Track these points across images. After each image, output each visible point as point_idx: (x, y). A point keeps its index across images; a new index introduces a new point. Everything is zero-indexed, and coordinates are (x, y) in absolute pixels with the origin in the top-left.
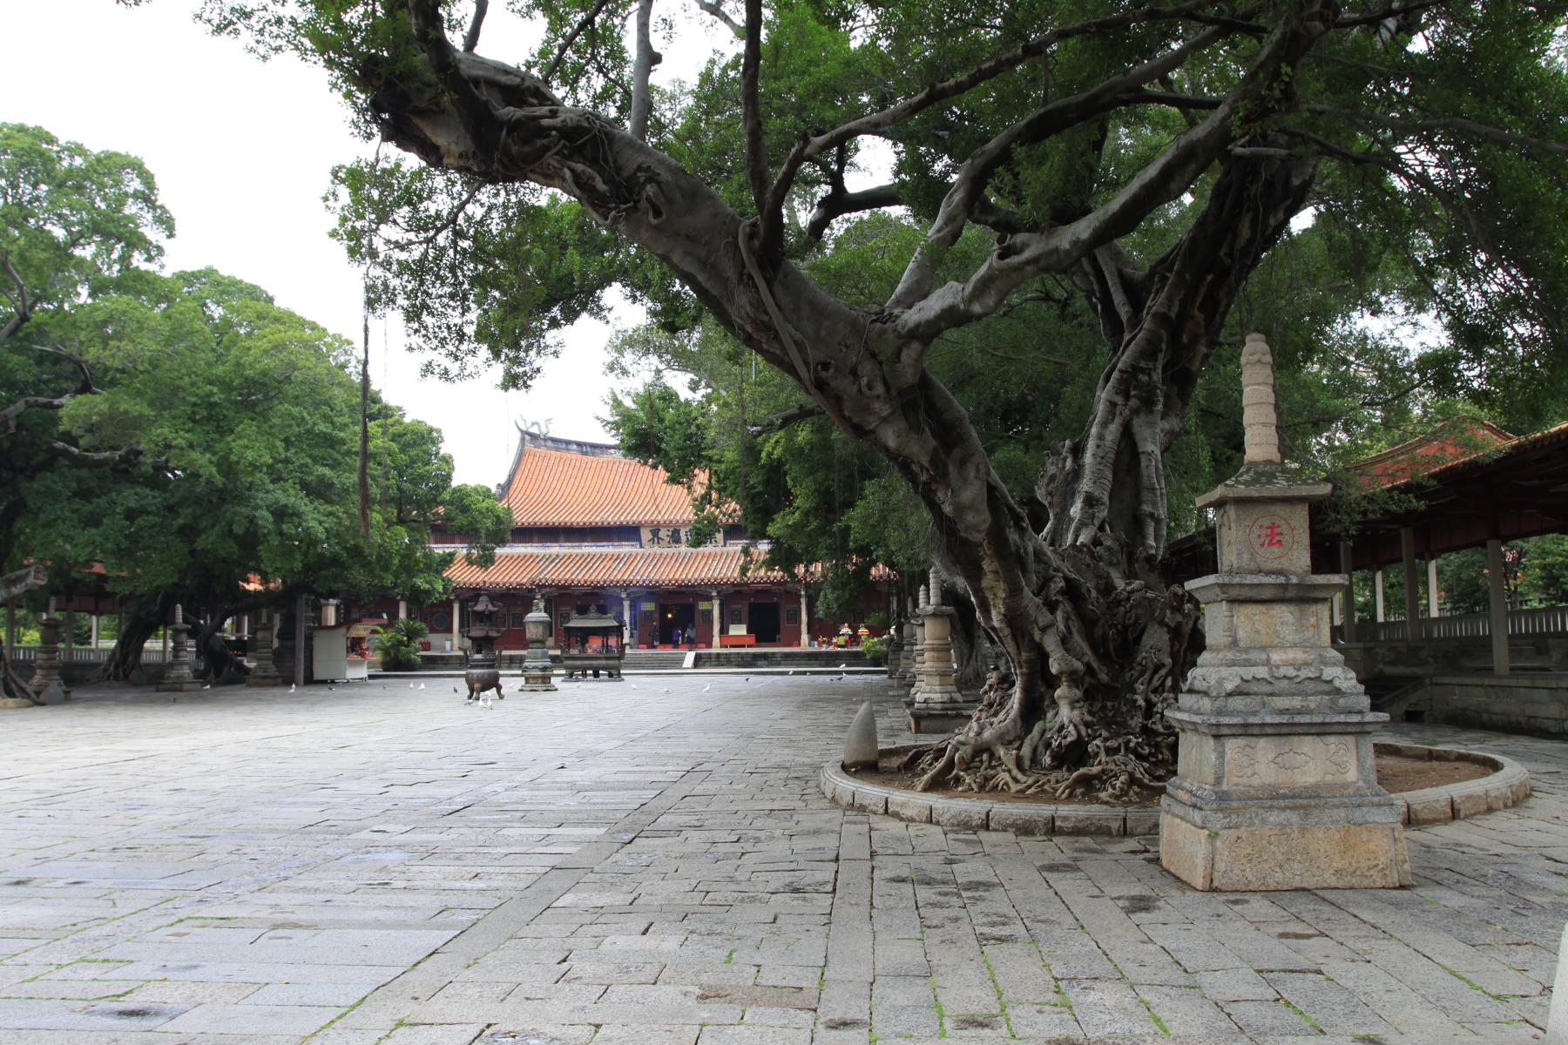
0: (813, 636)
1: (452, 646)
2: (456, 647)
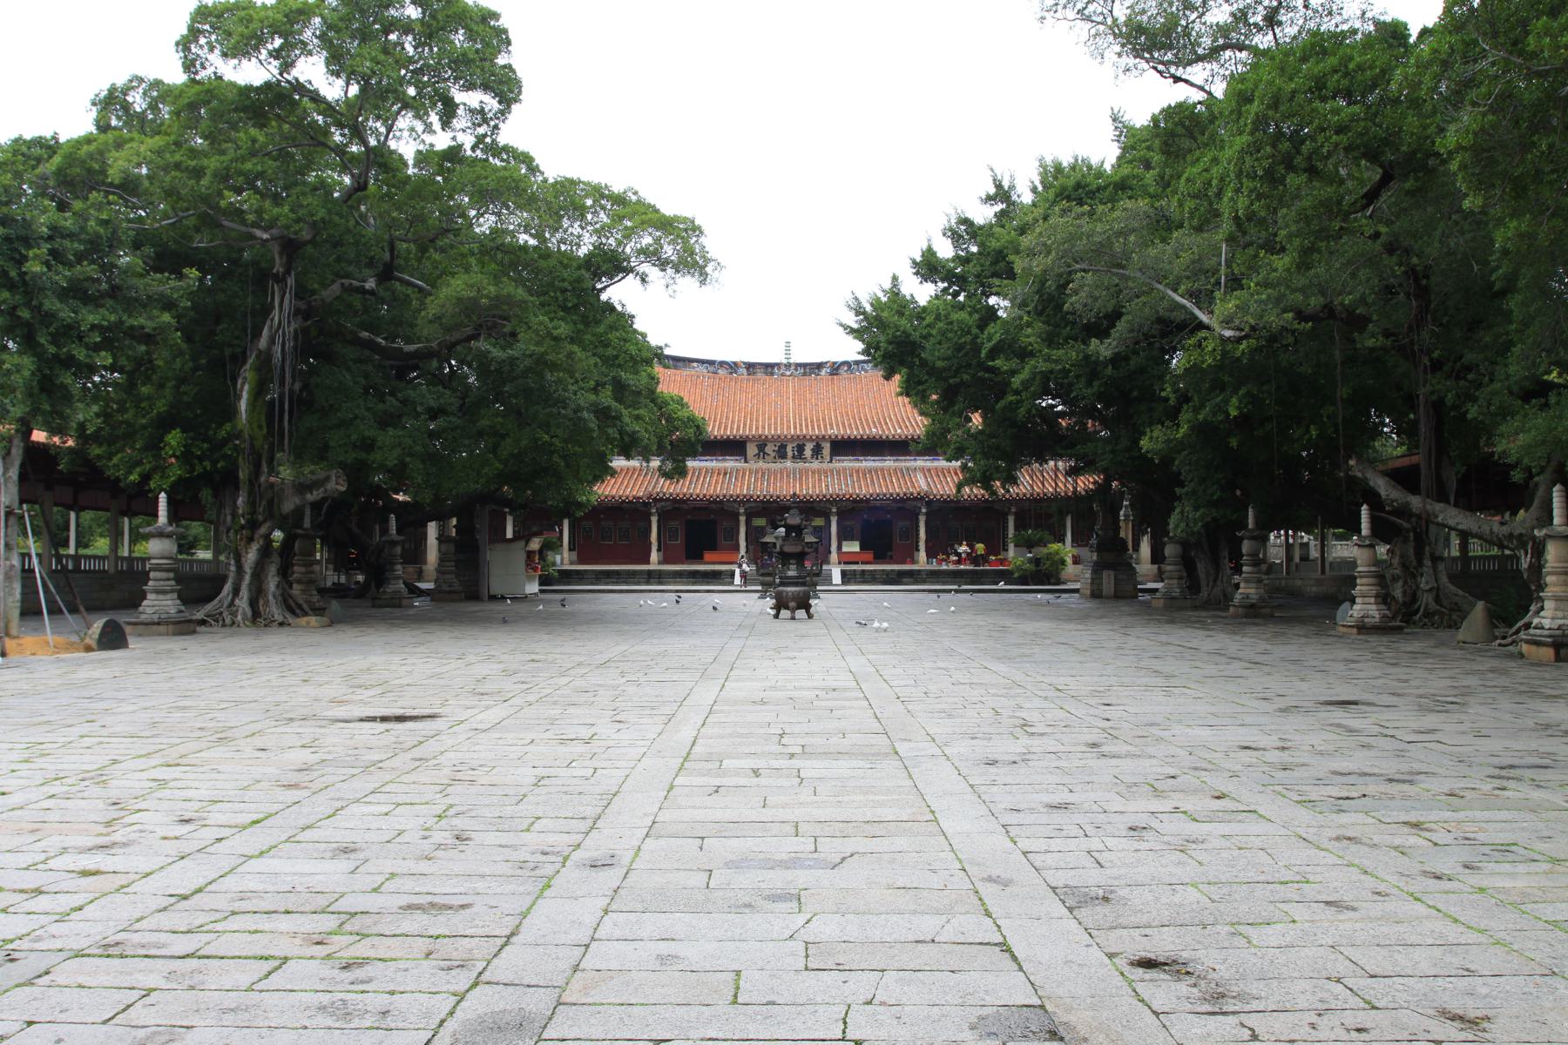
0: (931, 554)
1: (562, 559)
2: (566, 561)
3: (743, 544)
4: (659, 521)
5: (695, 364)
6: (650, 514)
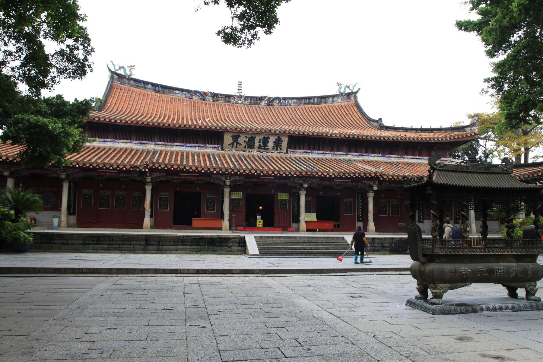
2: (64, 223)
3: (226, 212)
4: (152, 191)
5: (177, 92)
6: (145, 183)
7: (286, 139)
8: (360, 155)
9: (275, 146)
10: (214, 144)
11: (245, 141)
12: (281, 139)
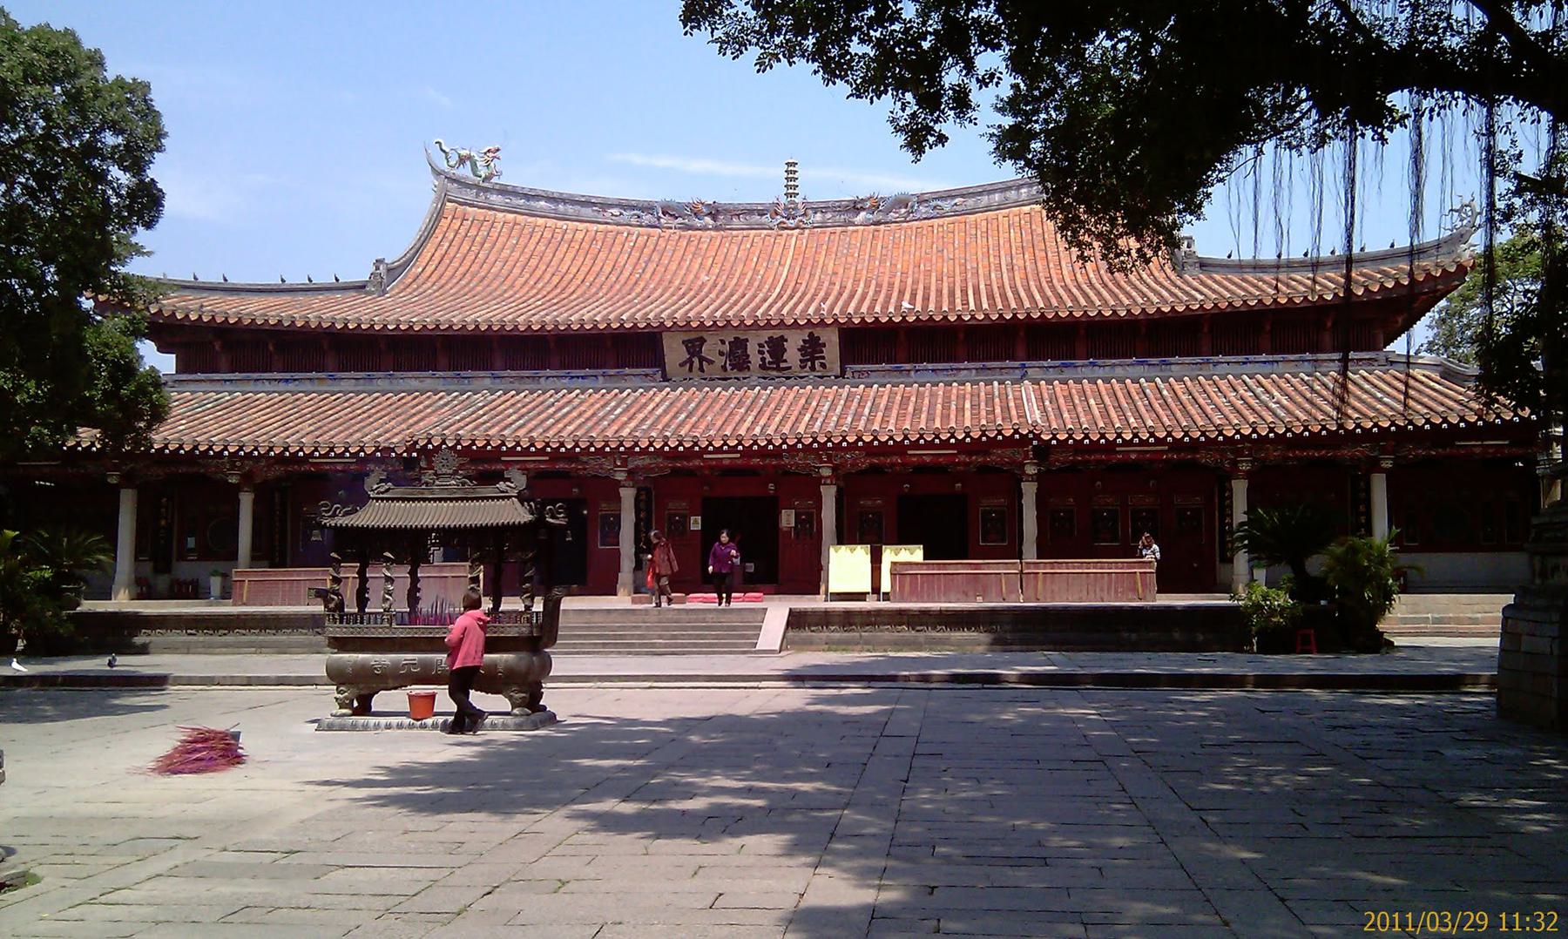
7: (835, 338)
8: (1066, 366)
9: (808, 360)
10: (644, 367)
11: (721, 354)
12: (819, 338)
